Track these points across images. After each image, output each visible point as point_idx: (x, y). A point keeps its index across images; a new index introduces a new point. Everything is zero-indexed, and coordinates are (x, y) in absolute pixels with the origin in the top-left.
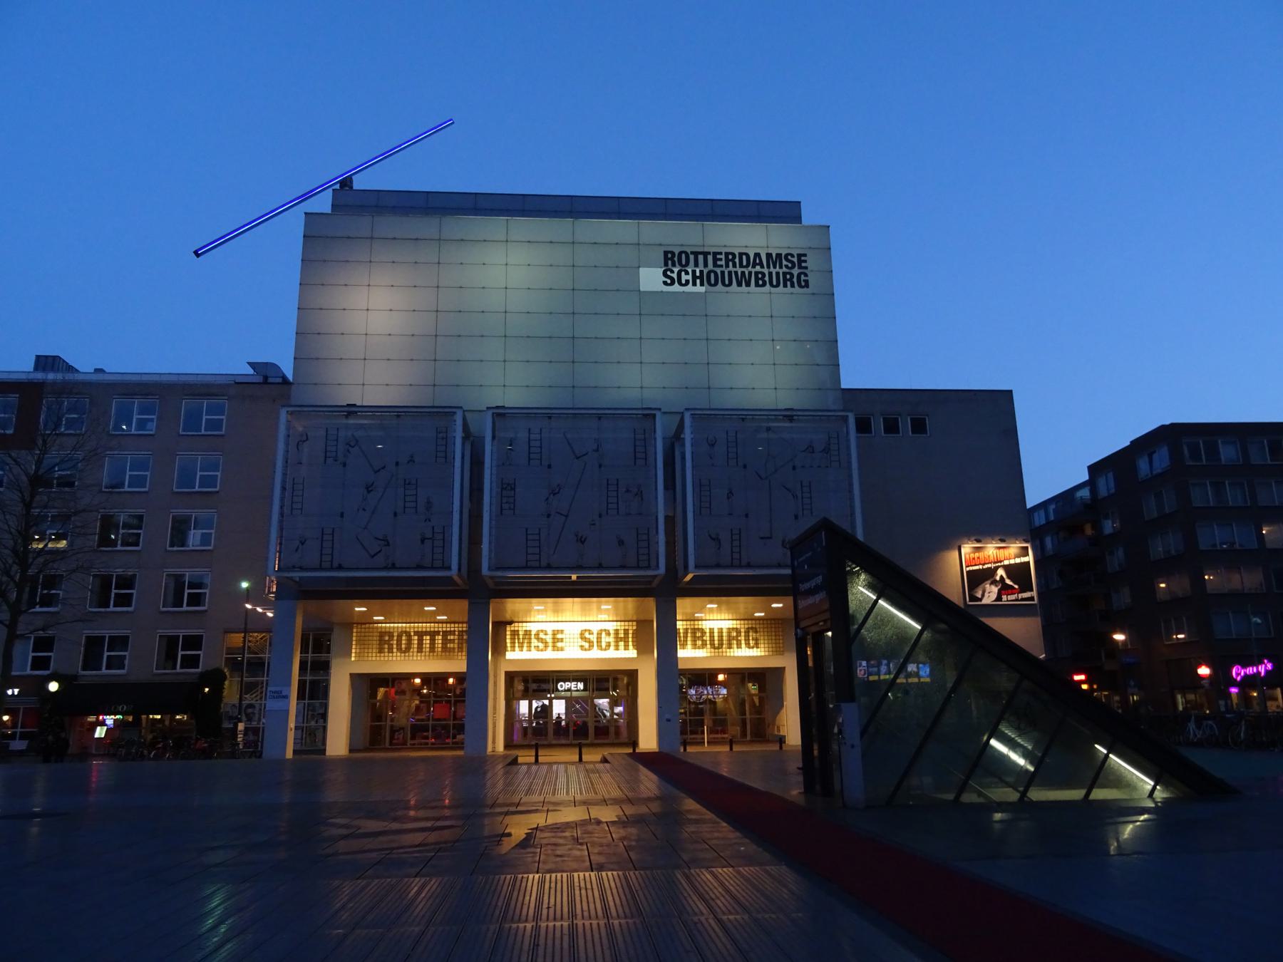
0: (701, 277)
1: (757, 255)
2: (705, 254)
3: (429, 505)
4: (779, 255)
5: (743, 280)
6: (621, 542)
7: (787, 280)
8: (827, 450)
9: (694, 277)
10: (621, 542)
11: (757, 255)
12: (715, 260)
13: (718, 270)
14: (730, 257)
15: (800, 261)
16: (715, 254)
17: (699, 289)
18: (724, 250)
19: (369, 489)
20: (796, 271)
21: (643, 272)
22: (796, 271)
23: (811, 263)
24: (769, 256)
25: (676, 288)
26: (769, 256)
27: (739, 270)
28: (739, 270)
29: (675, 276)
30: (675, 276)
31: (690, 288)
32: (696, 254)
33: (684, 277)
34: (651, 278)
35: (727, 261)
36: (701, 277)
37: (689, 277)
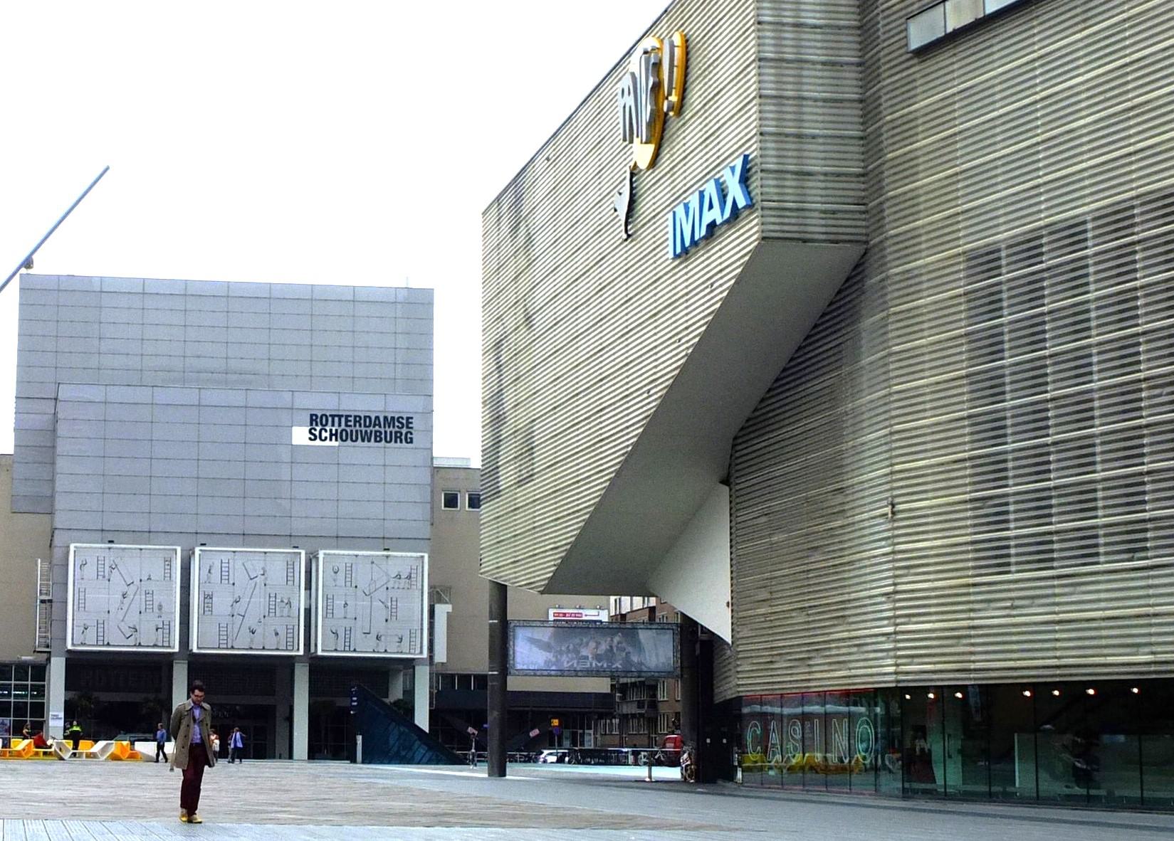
0: (336, 435)
1: (377, 418)
2: (340, 417)
3: (160, 607)
4: (393, 418)
5: (366, 437)
6: (277, 634)
7: (398, 437)
8: (409, 577)
9: (331, 435)
10: (277, 634)
11: (377, 418)
12: (347, 421)
13: (348, 429)
14: (357, 419)
15: (408, 423)
16: (347, 416)
17: (334, 443)
18: (353, 414)
19: (124, 596)
20: (404, 431)
21: (295, 430)
22: (404, 431)
23: (416, 424)
24: (386, 418)
25: (318, 442)
26: (386, 418)
27: (363, 429)
28: (363, 429)
29: (317, 433)
30: (317, 433)
31: (328, 443)
32: (333, 416)
33: (324, 434)
34: (300, 435)
35: (355, 422)
36: (336, 435)
37: (328, 435)
